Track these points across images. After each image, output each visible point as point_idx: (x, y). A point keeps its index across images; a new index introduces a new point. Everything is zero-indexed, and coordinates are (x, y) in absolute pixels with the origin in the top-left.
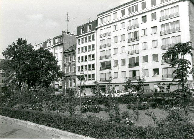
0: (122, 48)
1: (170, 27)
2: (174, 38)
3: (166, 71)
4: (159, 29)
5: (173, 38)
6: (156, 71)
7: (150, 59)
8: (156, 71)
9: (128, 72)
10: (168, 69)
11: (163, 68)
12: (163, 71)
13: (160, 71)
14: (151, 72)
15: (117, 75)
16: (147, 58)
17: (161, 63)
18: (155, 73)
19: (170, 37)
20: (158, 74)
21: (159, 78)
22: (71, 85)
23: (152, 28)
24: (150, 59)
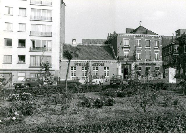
0: (7, 24)
1: (42, 14)
2: (45, 26)
3: (34, 58)
4: (29, 12)
5: (43, 26)
6: (22, 58)
7: (15, 43)
8: (22, 58)
9: (3, 56)
10: (36, 57)
11: (31, 56)
12: (30, 58)
13: (27, 59)
14: (15, 59)
15: (50, 58)
16: (25, 42)
17: (29, 50)
18: (19, 60)
19: (40, 25)
20: (25, 61)
21: (25, 66)
22: (166, 64)
23: (20, 8)
24: (15, 43)
